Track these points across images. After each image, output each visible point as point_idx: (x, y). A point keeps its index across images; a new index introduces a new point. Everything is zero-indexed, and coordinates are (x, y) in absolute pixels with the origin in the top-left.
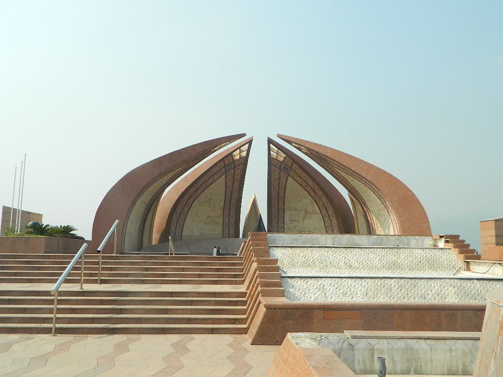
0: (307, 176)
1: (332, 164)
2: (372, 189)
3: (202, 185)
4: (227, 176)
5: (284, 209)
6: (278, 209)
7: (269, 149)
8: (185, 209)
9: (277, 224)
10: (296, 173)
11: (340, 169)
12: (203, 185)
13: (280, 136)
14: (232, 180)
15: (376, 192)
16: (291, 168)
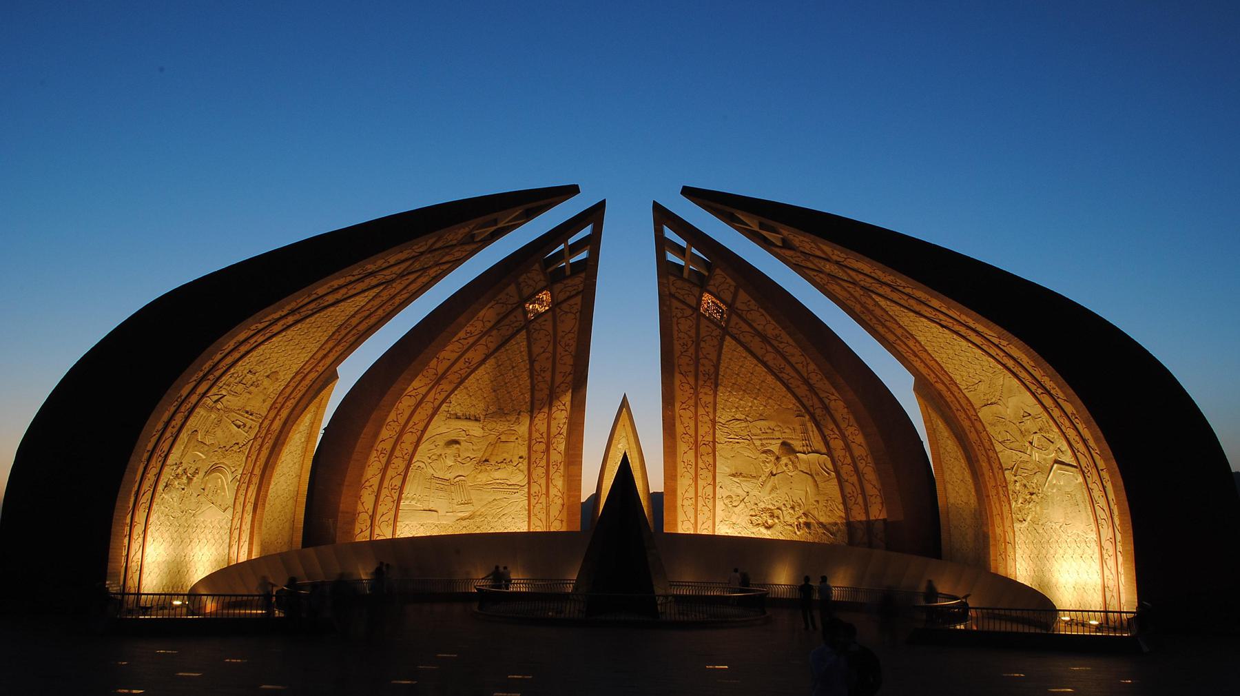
0: (783, 333)
1: (868, 282)
2: (1010, 364)
3: (453, 364)
4: (535, 335)
5: (714, 442)
6: (696, 441)
7: (662, 244)
8: (404, 438)
9: (692, 490)
10: (750, 326)
11: (895, 296)
12: (462, 360)
13: (688, 192)
14: (551, 348)
15: (1023, 374)
16: (730, 306)
